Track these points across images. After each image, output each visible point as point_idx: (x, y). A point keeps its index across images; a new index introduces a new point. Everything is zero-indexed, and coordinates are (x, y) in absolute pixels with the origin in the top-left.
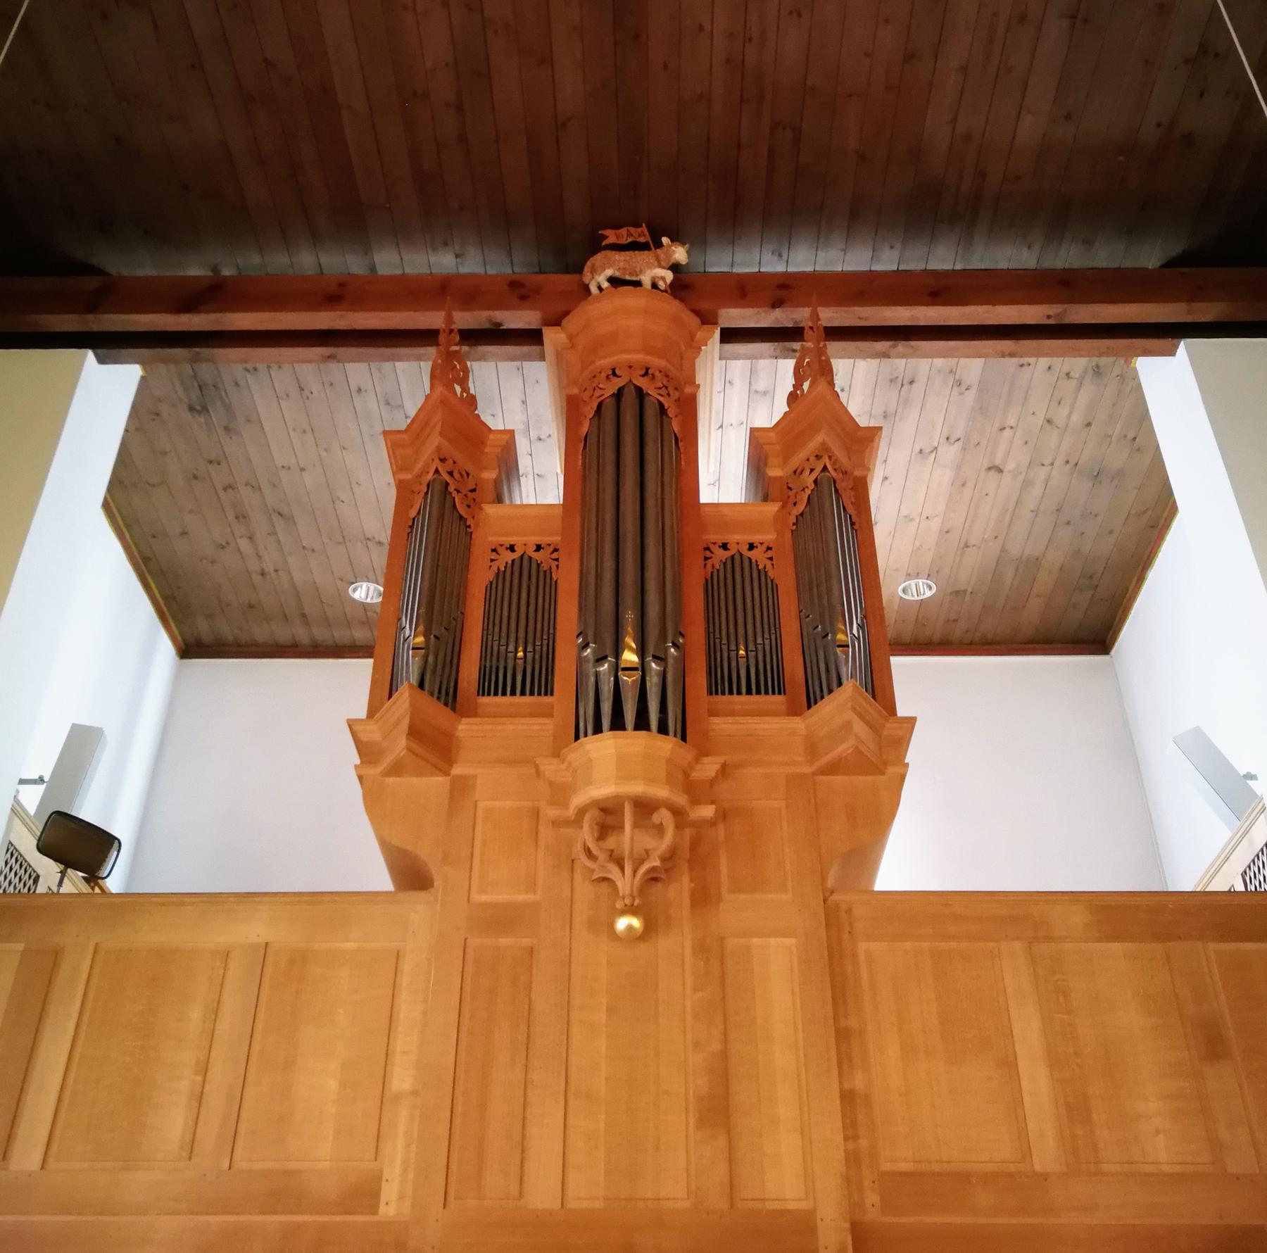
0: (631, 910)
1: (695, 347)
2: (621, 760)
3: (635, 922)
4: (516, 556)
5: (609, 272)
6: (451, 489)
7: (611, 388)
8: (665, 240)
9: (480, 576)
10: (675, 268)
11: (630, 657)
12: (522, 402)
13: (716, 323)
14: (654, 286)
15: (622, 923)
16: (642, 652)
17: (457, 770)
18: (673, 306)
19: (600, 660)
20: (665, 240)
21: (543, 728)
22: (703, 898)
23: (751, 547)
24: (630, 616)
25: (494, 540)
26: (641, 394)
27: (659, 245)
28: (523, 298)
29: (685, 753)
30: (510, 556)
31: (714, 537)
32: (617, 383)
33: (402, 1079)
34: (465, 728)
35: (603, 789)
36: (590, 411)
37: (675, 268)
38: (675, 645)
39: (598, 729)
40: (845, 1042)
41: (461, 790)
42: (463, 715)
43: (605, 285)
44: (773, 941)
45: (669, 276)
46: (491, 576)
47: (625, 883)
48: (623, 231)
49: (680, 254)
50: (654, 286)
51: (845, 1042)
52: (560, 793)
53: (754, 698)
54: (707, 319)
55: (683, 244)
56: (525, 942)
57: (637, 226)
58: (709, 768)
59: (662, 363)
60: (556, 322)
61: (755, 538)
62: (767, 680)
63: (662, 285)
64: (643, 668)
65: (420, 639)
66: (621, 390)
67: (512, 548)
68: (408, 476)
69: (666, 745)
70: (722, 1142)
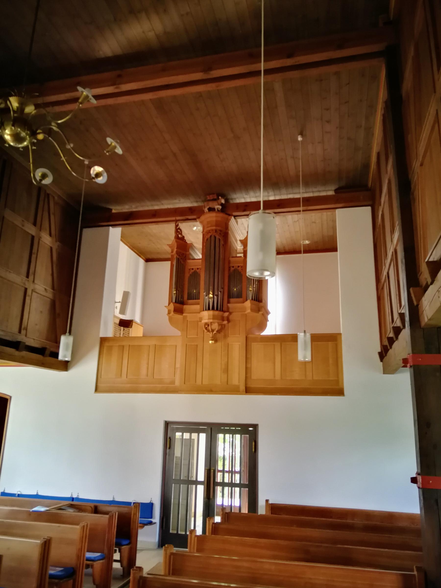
0: (212, 340)
1: (228, 220)
2: (209, 315)
3: (213, 342)
4: (194, 271)
5: (208, 207)
6: (180, 259)
7: (209, 236)
8: (220, 197)
9: (187, 275)
10: (222, 205)
11: (211, 296)
12: (194, 232)
13: (232, 215)
14: (218, 210)
15: (210, 342)
16: (213, 294)
17: (184, 314)
18: (221, 215)
19: (206, 296)
20: (220, 197)
21: (197, 307)
22: (226, 336)
23: (238, 267)
24: (211, 287)
25: (189, 267)
26: (215, 237)
27: (219, 199)
28: (192, 213)
29: (221, 313)
30: (192, 271)
31: (231, 265)
32: (210, 234)
33: (178, 365)
34: (185, 307)
35: (205, 321)
36: (206, 239)
37: (222, 205)
38: (220, 292)
39: (203, 311)
40: (247, 359)
41: (185, 318)
42: (185, 304)
43: (207, 211)
44: (237, 343)
45: (220, 207)
46: (189, 275)
47: (211, 335)
48: (211, 196)
49: (223, 201)
50: (218, 210)
51: (247, 359)
52: (201, 319)
53: (237, 299)
54: (230, 215)
55: (224, 198)
56: (196, 344)
57: (214, 194)
58: (226, 314)
59: (219, 228)
60: (199, 218)
61: (239, 265)
62: (239, 295)
63: (219, 209)
64: (214, 297)
65: (175, 292)
66: (211, 236)
67: (193, 269)
68: (172, 254)
69: (216, 313)
70: (226, 375)
